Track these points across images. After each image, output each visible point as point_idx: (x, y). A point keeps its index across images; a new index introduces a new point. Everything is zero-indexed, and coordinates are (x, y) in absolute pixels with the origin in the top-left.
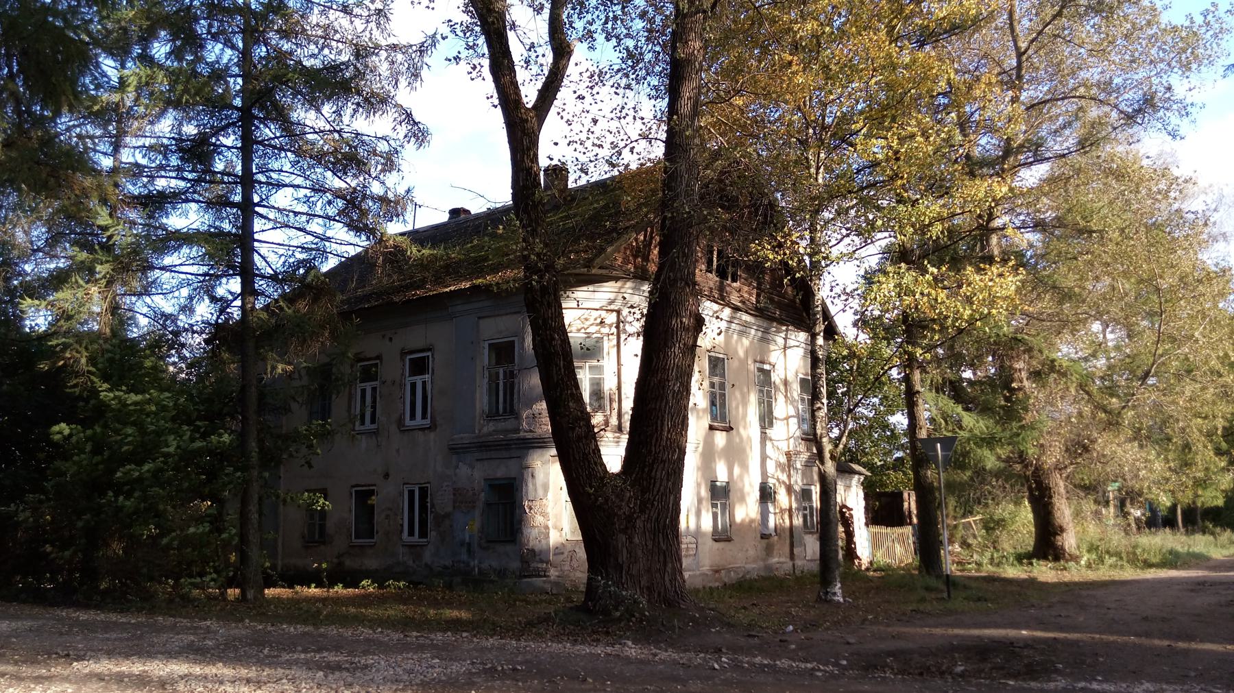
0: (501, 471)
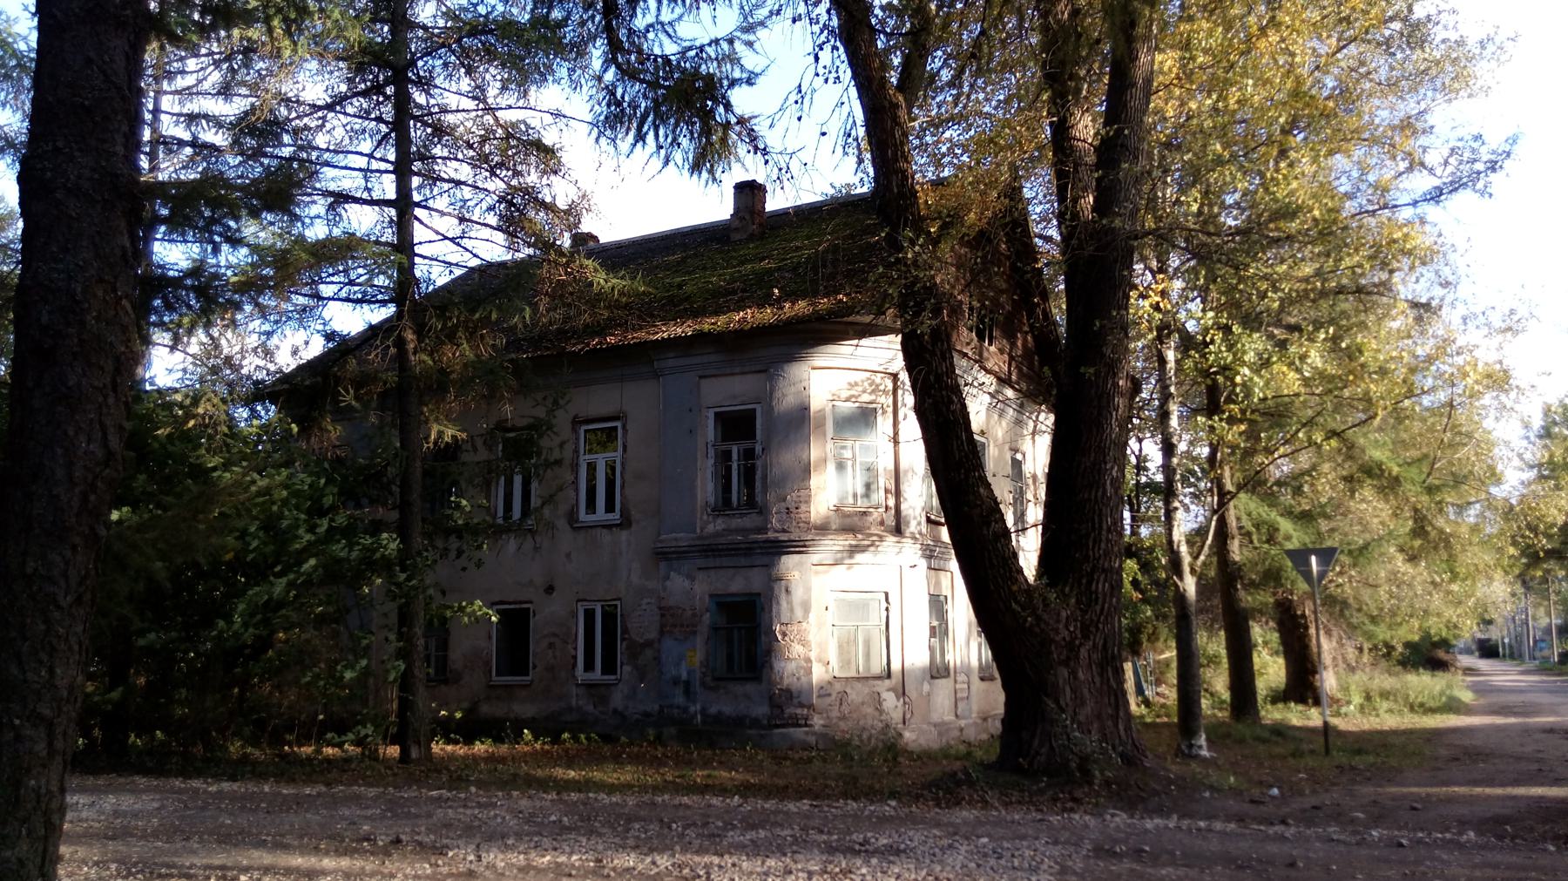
0: (738, 584)
